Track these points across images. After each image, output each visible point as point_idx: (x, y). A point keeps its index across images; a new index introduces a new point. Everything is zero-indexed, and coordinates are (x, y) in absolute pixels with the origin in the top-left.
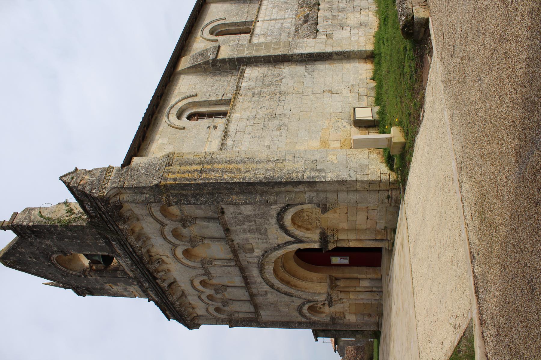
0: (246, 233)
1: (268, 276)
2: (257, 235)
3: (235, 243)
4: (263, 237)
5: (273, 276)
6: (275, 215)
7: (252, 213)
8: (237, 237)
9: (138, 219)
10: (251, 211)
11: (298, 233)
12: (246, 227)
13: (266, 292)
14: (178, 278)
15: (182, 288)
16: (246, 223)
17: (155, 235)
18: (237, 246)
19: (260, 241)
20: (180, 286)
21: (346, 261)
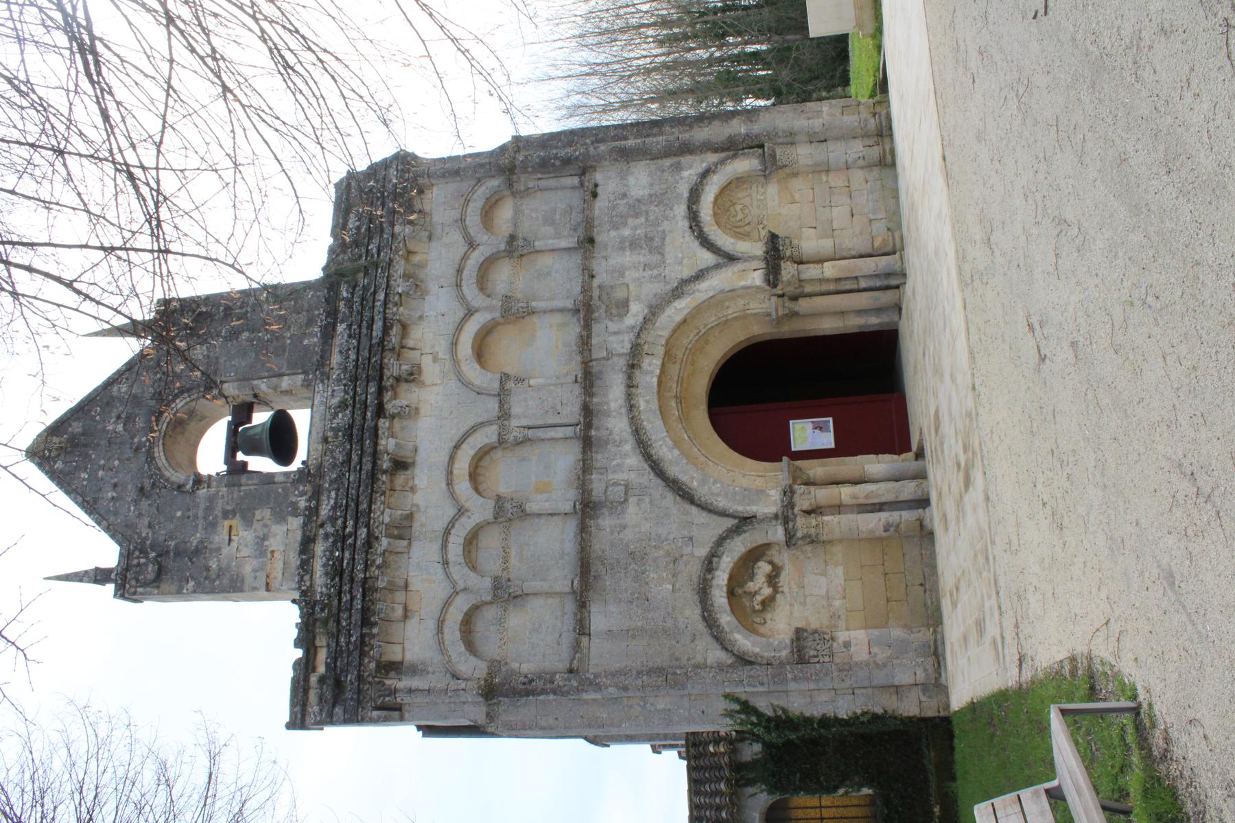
0: (623, 249)
1: (642, 405)
2: (642, 257)
3: (596, 282)
4: (656, 258)
5: (655, 405)
6: (686, 195)
7: (647, 192)
8: (604, 263)
9: (430, 238)
10: (644, 188)
11: (725, 241)
12: (626, 232)
13: (627, 487)
14: (421, 458)
15: (418, 498)
16: (630, 221)
17: (443, 281)
18: (596, 293)
19: (648, 273)
20: (413, 489)
21: (827, 440)
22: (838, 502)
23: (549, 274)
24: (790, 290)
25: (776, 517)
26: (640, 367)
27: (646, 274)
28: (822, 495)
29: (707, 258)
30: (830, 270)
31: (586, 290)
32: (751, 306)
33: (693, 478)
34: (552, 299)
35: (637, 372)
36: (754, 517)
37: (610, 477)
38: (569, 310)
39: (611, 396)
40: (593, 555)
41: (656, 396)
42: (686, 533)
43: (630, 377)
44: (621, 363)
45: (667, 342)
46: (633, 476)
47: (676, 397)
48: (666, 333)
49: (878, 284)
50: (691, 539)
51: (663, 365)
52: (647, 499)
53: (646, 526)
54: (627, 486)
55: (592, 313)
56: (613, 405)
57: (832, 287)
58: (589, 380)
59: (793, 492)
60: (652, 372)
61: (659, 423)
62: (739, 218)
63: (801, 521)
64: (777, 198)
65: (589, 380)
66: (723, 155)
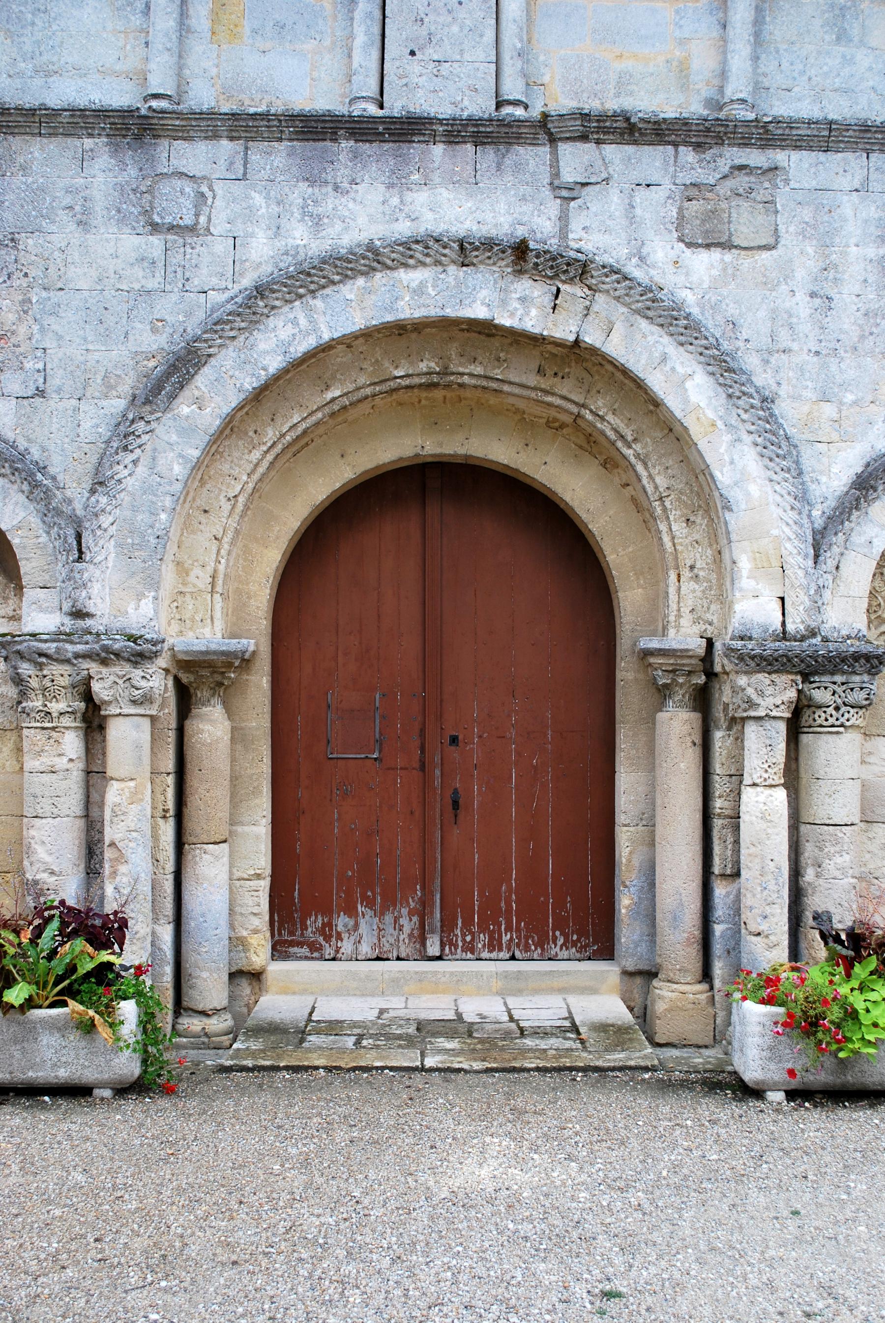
5: (408, 310)
22: (109, 773)
23: (842, 37)
24: (724, 695)
25: (79, 614)
26: (520, 272)
27: (801, 297)
28: (129, 739)
29: (835, 473)
30: (763, 808)
31: (769, 134)
32: (687, 586)
33: (200, 403)
34: (758, 39)
35: (506, 264)
36: (80, 559)
37: (218, 187)
38: (721, 90)
39: (444, 194)
40: (16, 142)
41: (434, 312)
42: (55, 382)
43: (489, 245)
44: (540, 223)
45: (593, 351)
46: (221, 247)
47: (445, 372)
48: (615, 347)
49: (718, 929)
50: (41, 393)
51: (536, 341)
52: (152, 284)
53: (81, 276)
54: (192, 229)
55: (698, 147)
56: (420, 199)
57: (718, 804)
58: (491, 133)
59: (139, 658)
60: (504, 303)
61: (357, 320)
63: (61, 675)
65: (491, 133)
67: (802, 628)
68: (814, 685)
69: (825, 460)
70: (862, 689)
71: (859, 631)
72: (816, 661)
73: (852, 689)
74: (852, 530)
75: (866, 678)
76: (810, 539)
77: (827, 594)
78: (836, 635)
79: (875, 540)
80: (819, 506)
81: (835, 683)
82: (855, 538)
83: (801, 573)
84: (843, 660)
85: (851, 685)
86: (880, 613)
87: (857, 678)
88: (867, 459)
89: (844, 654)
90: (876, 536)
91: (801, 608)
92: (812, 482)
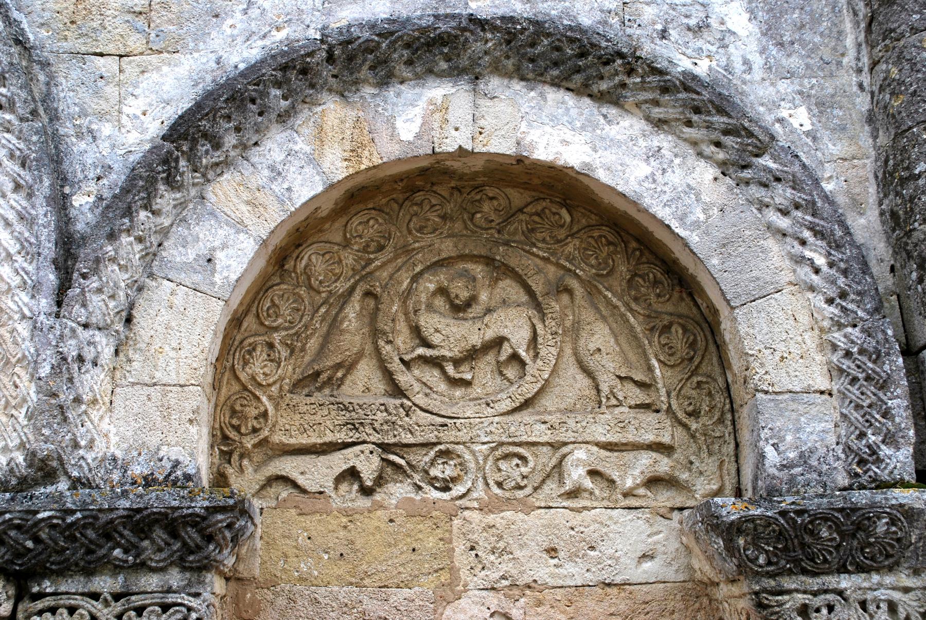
62: (429, 322)
64: (575, 572)
66: (867, 225)
67: (20, 458)
68: (40, 605)
69: (111, 91)
70: (165, 608)
71: (176, 464)
72: (37, 540)
73: (140, 611)
74: (165, 232)
75: (175, 578)
76: (49, 249)
77: (93, 381)
78: (116, 476)
79: (220, 255)
80: (92, 187)
81: (95, 596)
82: (173, 253)
83: (23, 329)
84: (108, 533)
85: (137, 601)
86: (265, 433)
87: (152, 582)
88: (208, 83)
89: (103, 518)
90: (224, 246)
91: (21, 415)
92: (79, 136)
